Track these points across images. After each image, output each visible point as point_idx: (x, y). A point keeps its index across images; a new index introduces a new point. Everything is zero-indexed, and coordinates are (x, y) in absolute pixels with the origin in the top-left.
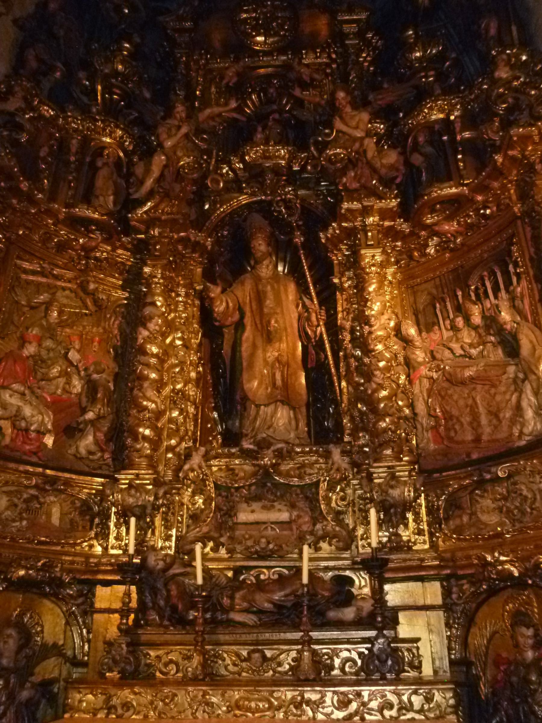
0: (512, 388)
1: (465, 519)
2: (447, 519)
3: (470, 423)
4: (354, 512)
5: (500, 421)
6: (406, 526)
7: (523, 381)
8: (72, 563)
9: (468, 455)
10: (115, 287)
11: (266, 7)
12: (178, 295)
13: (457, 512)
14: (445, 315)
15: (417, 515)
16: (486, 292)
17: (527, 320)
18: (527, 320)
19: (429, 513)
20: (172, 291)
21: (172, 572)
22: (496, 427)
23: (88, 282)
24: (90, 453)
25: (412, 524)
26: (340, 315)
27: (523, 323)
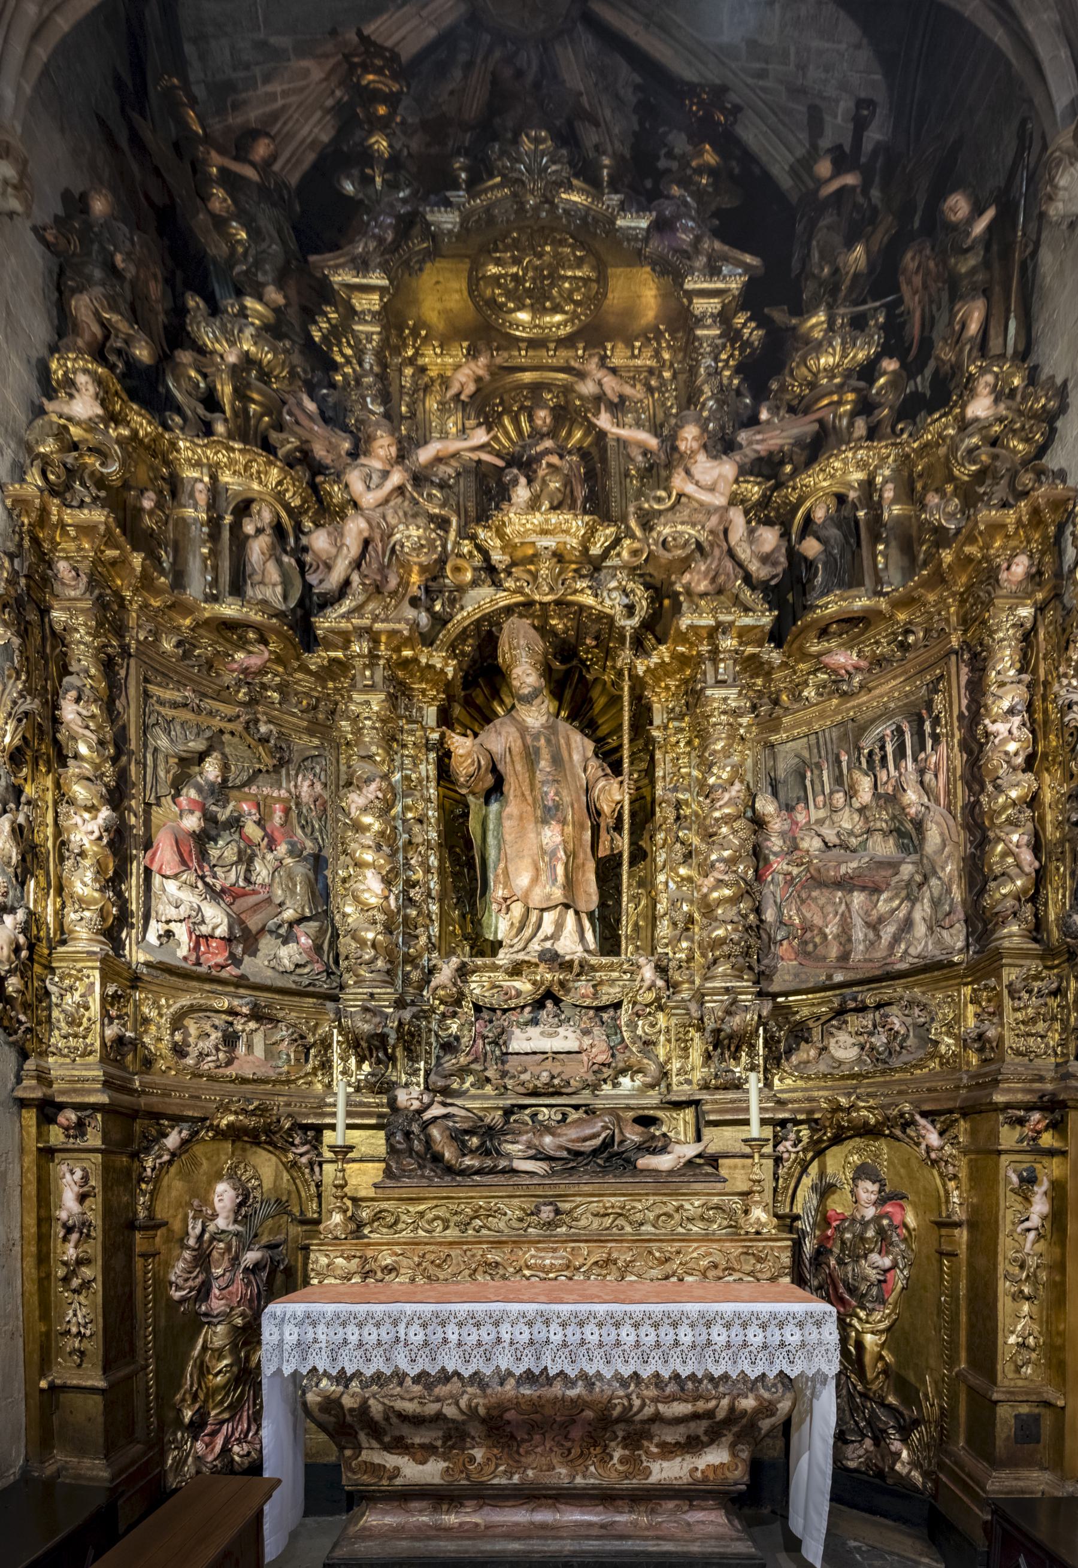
0: (903, 894)
1: (813, 1053)
2: (789, 1052)
3: (837, 937)
4: (669, 1041)
5: (879, 937)
6: (737, 1059)
7: (920, 886)
8: (288, 1105)
9: (830, 977)
10: (297, 730)
11: (540, 256)
12: (404, 746)
13: (803, 1045)
14: (818, 788)
15: (752, 1046)
16: (884, 758)
17: (937, 801)
18: (937, 801)
19: (766, 1044)
20: (394, 739)
21: (428, 1115)
22: (872, 943)
23: (257, 721)
24: (298, 966)
25: (744, 1058)
26: (660, 785)
27: (932, 805)
